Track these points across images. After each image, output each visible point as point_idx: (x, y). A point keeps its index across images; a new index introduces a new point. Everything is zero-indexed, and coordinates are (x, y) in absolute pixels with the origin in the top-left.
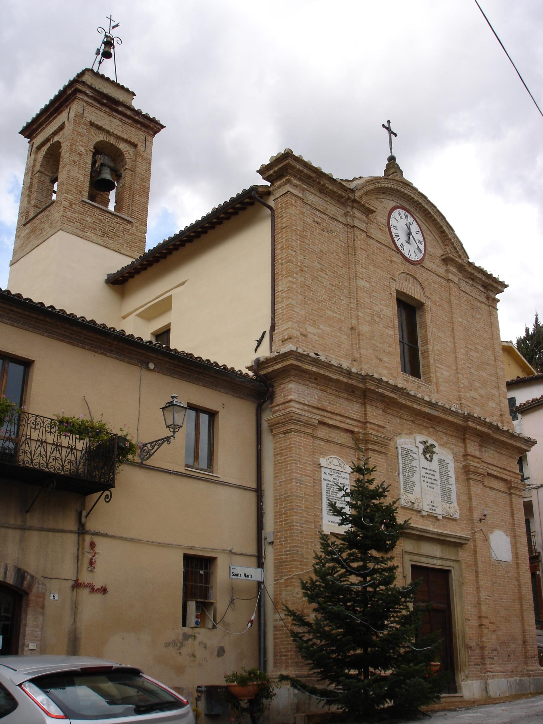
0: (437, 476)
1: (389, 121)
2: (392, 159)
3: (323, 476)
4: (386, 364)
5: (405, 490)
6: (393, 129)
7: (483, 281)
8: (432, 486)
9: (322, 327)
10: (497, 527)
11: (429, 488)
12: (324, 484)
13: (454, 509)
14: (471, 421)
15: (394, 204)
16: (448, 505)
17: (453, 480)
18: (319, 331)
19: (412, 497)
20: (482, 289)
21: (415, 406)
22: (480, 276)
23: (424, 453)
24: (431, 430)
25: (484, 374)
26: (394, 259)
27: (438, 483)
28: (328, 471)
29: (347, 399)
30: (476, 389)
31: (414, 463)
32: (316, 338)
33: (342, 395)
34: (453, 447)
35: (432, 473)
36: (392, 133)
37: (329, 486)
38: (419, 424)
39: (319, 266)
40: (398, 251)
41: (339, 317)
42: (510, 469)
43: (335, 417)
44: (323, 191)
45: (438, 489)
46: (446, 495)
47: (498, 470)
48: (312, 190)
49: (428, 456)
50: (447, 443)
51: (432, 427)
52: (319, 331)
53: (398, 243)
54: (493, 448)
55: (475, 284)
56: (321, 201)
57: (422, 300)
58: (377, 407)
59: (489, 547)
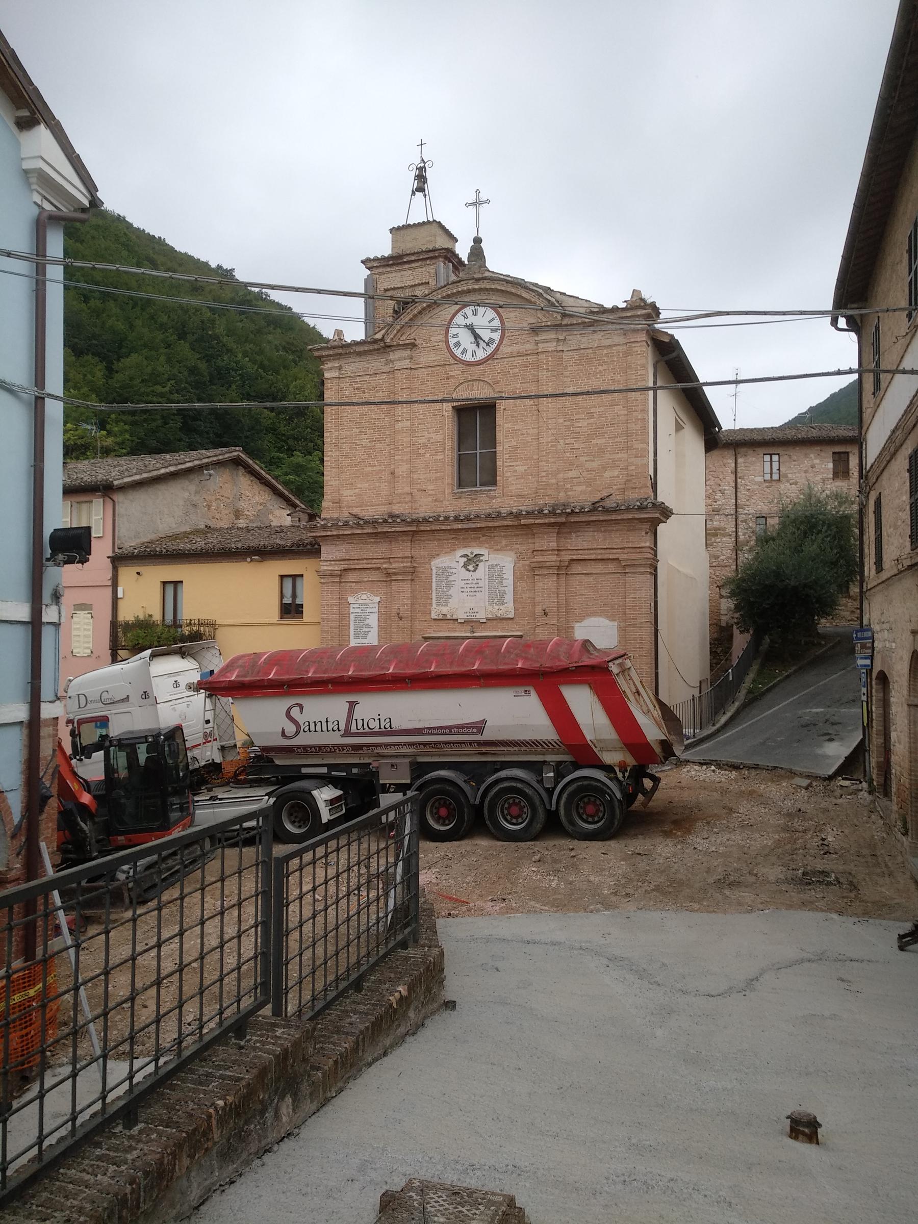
0: (484, 583)
3: (352, 610)
5: (438, 604)
9: (359, 486)
12: (352, 617)
13: (508, 608)
18: (357, 491)
19: (445, 610)
23: (465, 566)
26: (451, 374)
28: (357, 606)
29: (375, 543)
31: (451, 578)
32: (354, 498)
35: (475, 581)
37: (356, 617)
38: (464, 539)
41: (379, 468)
42: (630, 545)
43: (361, 562)
46: (497, 597)
49: (471, 567)
50: (506, 546)
52: (357, 491)
53: (458, 352)
56: (364, 364)
58: (403, 541)
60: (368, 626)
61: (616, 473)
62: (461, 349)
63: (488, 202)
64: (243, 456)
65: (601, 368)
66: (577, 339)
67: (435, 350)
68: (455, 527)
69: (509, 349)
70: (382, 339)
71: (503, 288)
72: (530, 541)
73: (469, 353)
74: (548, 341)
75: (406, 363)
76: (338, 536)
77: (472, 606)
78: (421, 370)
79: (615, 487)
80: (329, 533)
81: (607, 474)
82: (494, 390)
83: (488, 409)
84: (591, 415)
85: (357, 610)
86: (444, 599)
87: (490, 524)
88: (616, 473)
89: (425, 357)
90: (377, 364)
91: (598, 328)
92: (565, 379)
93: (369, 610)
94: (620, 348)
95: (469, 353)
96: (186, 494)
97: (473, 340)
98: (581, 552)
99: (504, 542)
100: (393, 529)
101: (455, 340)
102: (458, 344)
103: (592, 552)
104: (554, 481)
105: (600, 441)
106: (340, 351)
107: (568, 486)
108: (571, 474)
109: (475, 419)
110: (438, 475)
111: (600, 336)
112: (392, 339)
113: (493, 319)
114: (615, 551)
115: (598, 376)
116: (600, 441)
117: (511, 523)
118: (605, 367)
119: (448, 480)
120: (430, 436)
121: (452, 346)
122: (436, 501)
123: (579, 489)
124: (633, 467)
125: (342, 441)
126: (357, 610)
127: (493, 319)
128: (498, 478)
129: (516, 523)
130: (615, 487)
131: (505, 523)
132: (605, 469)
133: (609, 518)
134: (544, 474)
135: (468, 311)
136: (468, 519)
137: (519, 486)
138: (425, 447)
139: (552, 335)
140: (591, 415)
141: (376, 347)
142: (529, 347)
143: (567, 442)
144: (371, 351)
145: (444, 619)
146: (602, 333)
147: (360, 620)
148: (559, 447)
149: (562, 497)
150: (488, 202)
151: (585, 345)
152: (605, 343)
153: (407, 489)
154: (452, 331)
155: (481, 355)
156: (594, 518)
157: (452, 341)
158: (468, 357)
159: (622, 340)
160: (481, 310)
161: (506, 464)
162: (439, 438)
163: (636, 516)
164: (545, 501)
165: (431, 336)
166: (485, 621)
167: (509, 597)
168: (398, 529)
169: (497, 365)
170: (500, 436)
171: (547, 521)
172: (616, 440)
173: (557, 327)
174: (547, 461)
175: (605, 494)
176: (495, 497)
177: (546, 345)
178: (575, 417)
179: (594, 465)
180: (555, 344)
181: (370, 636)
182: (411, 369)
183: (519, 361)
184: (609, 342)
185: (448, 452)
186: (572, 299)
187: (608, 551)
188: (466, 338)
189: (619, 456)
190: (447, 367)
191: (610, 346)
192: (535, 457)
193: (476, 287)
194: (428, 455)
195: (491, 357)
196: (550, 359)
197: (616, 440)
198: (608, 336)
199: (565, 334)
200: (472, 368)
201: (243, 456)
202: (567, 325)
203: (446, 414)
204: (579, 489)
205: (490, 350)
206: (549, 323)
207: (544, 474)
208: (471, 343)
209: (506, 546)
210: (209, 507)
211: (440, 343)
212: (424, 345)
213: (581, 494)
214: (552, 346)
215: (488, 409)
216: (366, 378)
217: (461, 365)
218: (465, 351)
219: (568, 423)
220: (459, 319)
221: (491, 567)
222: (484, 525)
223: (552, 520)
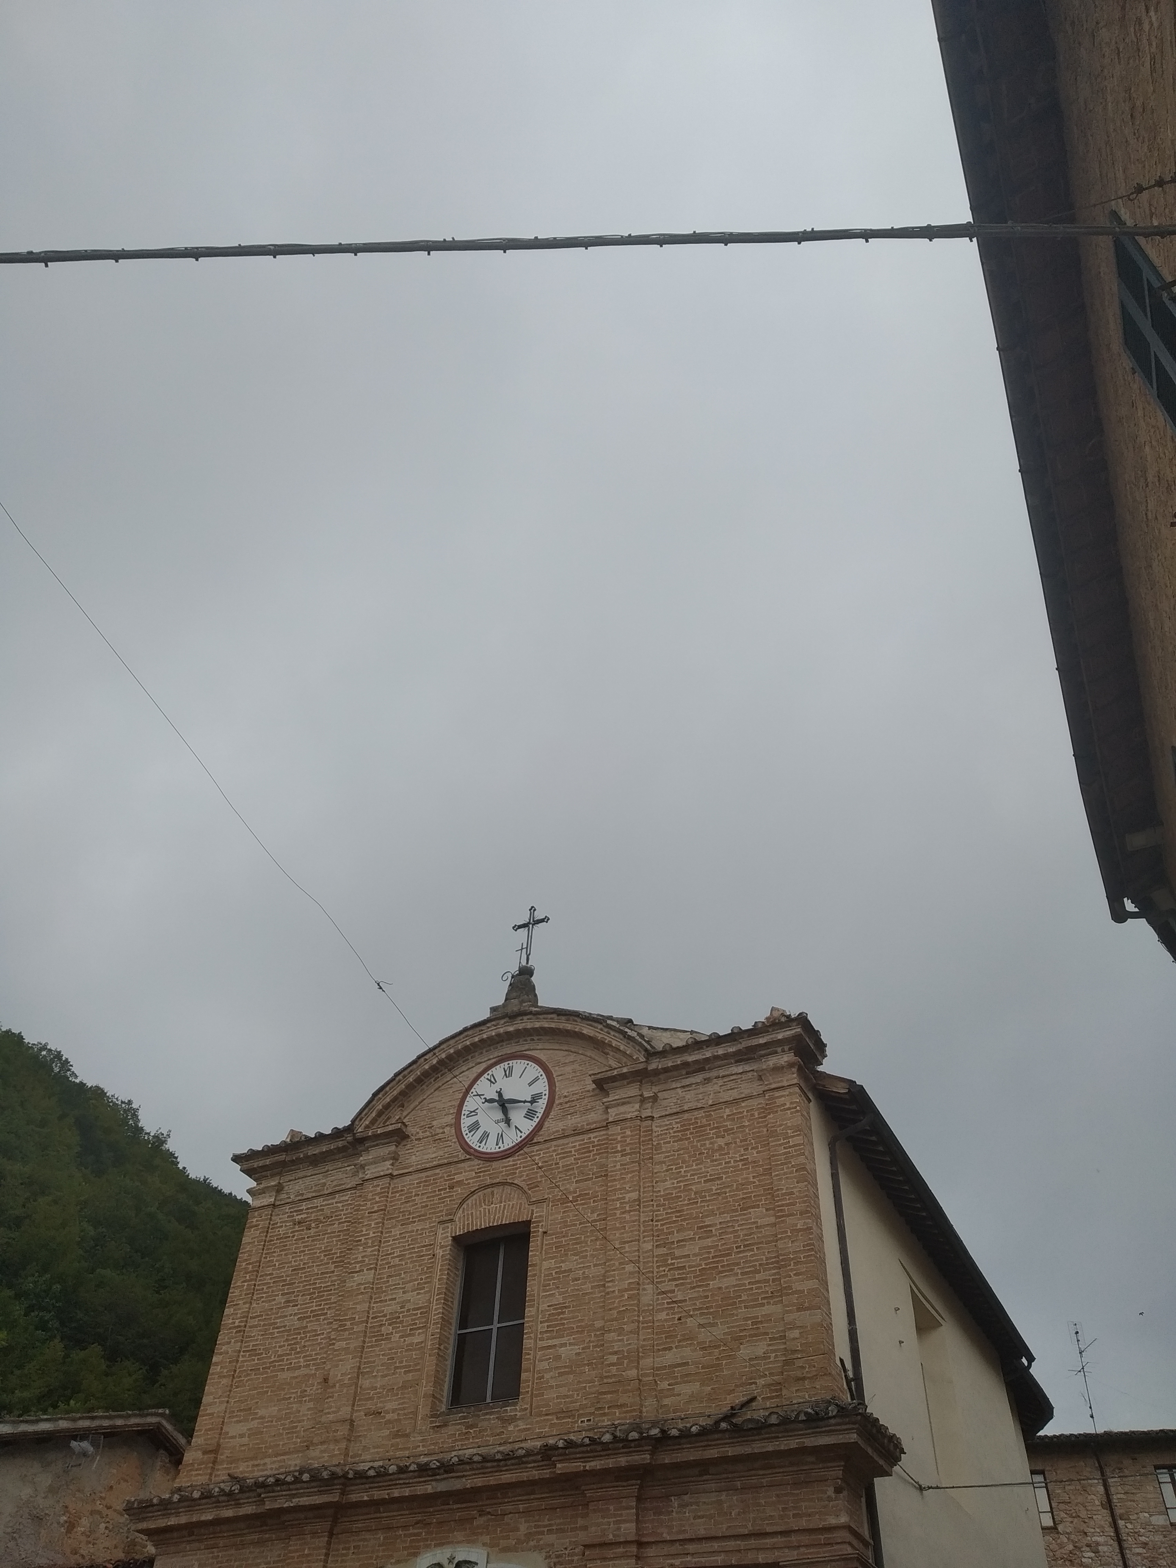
2: (526, 972)
4: (388, 1417)
7: (734, 1054)
9: (261, 1412)
14: (560, 1461)
18: (254, 1424)
21: (396, 1493)
24: (481, 1521)
26: (457, 1178)
29: (260, 1543)
32: (245, 1440)
33: (249, 1538)
38: (440, 1523)
41: (303, 1371)
42: (803, 1523)
44: (315, 1161)
47: (731, 1544)
48: (301, 1174)
51: (482, 1513)
52: (254, 1424)
53: (472, 1140)
54: (713, 1486)
56: (320, 1179)
58: (314, 1534)
61: (761, 1348)
62: (479, 1133)
63: (545, 920)
64: (169, 1427)
65: (721, 1142)
66: (676, 1095)
67: (436, 1140)
68: (420, 1490)
69: (561, 1125)
71: (553, 1025)
72: (580, 1522)
73: (492, 1139)
74: (626, 1103)
75: (386, 1167)
76: (191, 1528)
78: (408, 1178)
79: (761, 1382)
80: (172, 1521)
81: (745, 1352)
82: (528, 1198)
83: (515, 1239)
84: (705, 1231)
87: (492, 1480)
88: (761, 1348)
89: (417, 1155)
90: (340, 1175)
91: (714, 1074)
92: (657, 1168)
94: (754, 1103)
95: (492, 1139)
96: (26, 1492)
97: (500, 1116)
98: (691, 1548)
99: (523, 1528)
100: (295, 1501)
101: (472, 1120)
102: (475, 1127)
103: (716, 1545)
104: (632, 1373)
105: (728, 1282)
106: (282, 1157)
107: (664, 1385)
108: (670, 1358)
109: (492, 1260)
110: (410, 1376)
111: (716, 1087)
112: (367, 1127)
113: (537, 1079)
114: (769, 1541)
115: (717, 1156)
116: (728, 1282)
117: (535, 1474)
118: (728, 1139)
119: (426, 1387)
120: (407, 1296)
121: (465, 1130)
122: (396, 1435)
123: (687, 1389)
124: (796, 1333)
125: (252, 1322)
127: (537, 1079)
128: (524, 1376)
129: (546, 1473)
130: (761, 1382)
131: (524, 1476)
132: (739, 1340)
133: (747, 1450)
134: (614, 1359)
135: (498, 1071)
136: (447, 1468)
137: (564, 1391)
138: (394, 1320)
139: (632, 1091)
140: (705, 1231)
141: (340, 1144)
142: (595, 1117)
143: (664, 1287)
144: (330, 1153)
146: (720, 1082)
148: (645, 1300)
149: (649, 1409)
150: (545, 920)
151: (693, 1105)
152: (726, 1096)
153: (345, 1411)
154: (471, 1103)
155: (511, 1139)
156: (713, 1453)
157: (466, 1122)
158: (490, 1147)
159: (756, 1088)
160: (518, 1065)
161: (540, 1344)
162: (417, 1299)
163: (810, 1442)
164: (612, 1420)
165: (434, 1119)
168: (304, 1501)
169: (539, 1154)
170: (533, 1287)
171: (610, 1463)
172: (758, 1277)
173: (641, 1076)
174: (620, 1331)
175: (739, 1398)
176: (513, 1419)
177: (622, 1109)
178: (676, 1237)
179: (720, 1331)
180: (637, 1106)
182: (391, 1176)
183: (574, 1143)
184: (734, 1094)
185: (434, 1328)
186: (668, 1034)
187: (753, 1542)
188: (489, 1119)
189: (767, 1310)
190: (452, 1169)
191: (735, 1102)
192: (598, 1324)
193: (511, 1029)
194: (396, 1337)
195: (529, 1141)
196: (628, 1133)
197: (758, 1277)
198: (732, 1084)
199: (655, 1089)
200: (495, 1164)
201: (169, 1427)
202: (656, 1072)
203: (439, 1252)
204: (687, 1389)
205: (528, 1126)
206: (625, 1070)
207: (614, 1359)
208: (497, 1122)
209: (529, 1536)
210: (71, 1526)
211: (447, 1130)
212: (421, 1135)
213: (689, 1401)
214: (631, 1110)
215: (515, 1239)
216: (317, 1202)
217: (476, 1162)
218: (485, 1136)
219: (663, 1251)
220: (483, 1087)
222: (479, 1482)
223: (623, 1461)
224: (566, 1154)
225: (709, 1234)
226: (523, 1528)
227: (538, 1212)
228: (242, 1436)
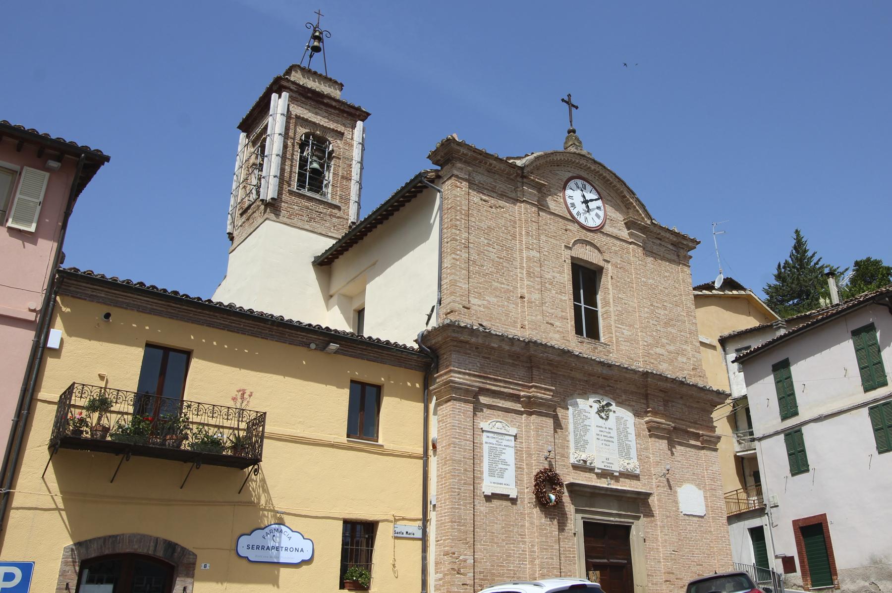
0: (614, 433)
1: (569, 95)
5: (577, 448)
6: (573, 101)
8: (608, 443)
9: (487, 298)
10: (688, 481)
11: (604, 446)
12: (486, 448)
13: (632, 464)
15: (570, 175)
16: (627, 461)
17: (632, 437)
18: (485, 303)
20: (671, 247)
22: (668, 235)
23: (599, 412)
25: (673, 331)
26: (569, 227)
27: (615, 440)
28: (492, 435)
30: (663, 346)
31: (587, 422)
32: (482, 309)
34: (633, 404)
35: (607, 430)
36: (573, 106)
37: (491, 449)
39: (486, 241)
40: (574, 220)
41: (506, 287)
45: (614, 446)
46: (624, 451)
49: (603, 415)
50: (626, 400)
52: (485, 303)
53: (574, 212)
55: (663, 243)
56: (490, 180)
57: (601, 263)
59: (676, 502)
60: (504, 462)
70: (522, 168)
77: (607, 456)
85: (494, 441)
86: (581, 445)
93: (505, 443)
99: (624, 397)
126: (494, 441)
145: (583, 467)
147: (495, 453)
166: (617, 474)
167: (633, 453)
181: (506, 474)
209: (626, 400)
221: (618, 418)
224: (615, 245)
225: (666, 309)
226: (624, 397)
227: (609, 267)
228: (480, 306)
